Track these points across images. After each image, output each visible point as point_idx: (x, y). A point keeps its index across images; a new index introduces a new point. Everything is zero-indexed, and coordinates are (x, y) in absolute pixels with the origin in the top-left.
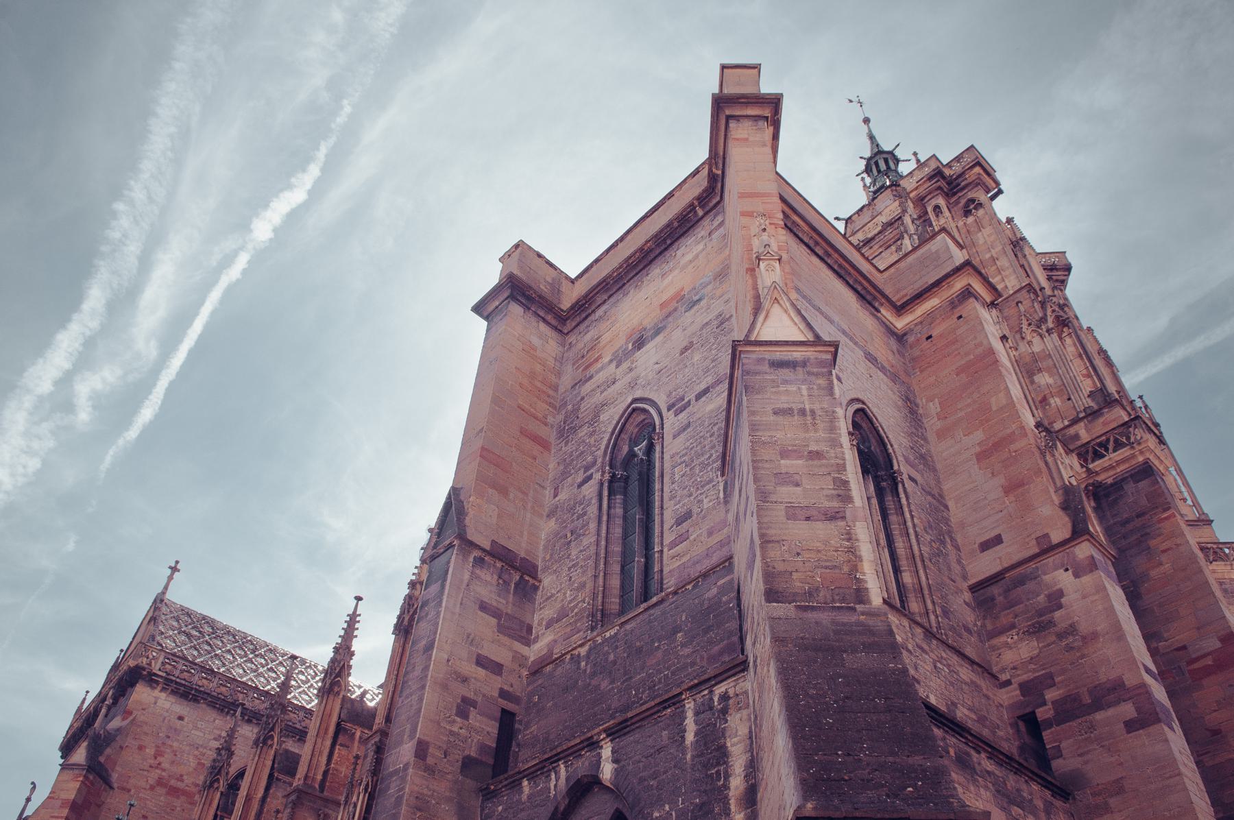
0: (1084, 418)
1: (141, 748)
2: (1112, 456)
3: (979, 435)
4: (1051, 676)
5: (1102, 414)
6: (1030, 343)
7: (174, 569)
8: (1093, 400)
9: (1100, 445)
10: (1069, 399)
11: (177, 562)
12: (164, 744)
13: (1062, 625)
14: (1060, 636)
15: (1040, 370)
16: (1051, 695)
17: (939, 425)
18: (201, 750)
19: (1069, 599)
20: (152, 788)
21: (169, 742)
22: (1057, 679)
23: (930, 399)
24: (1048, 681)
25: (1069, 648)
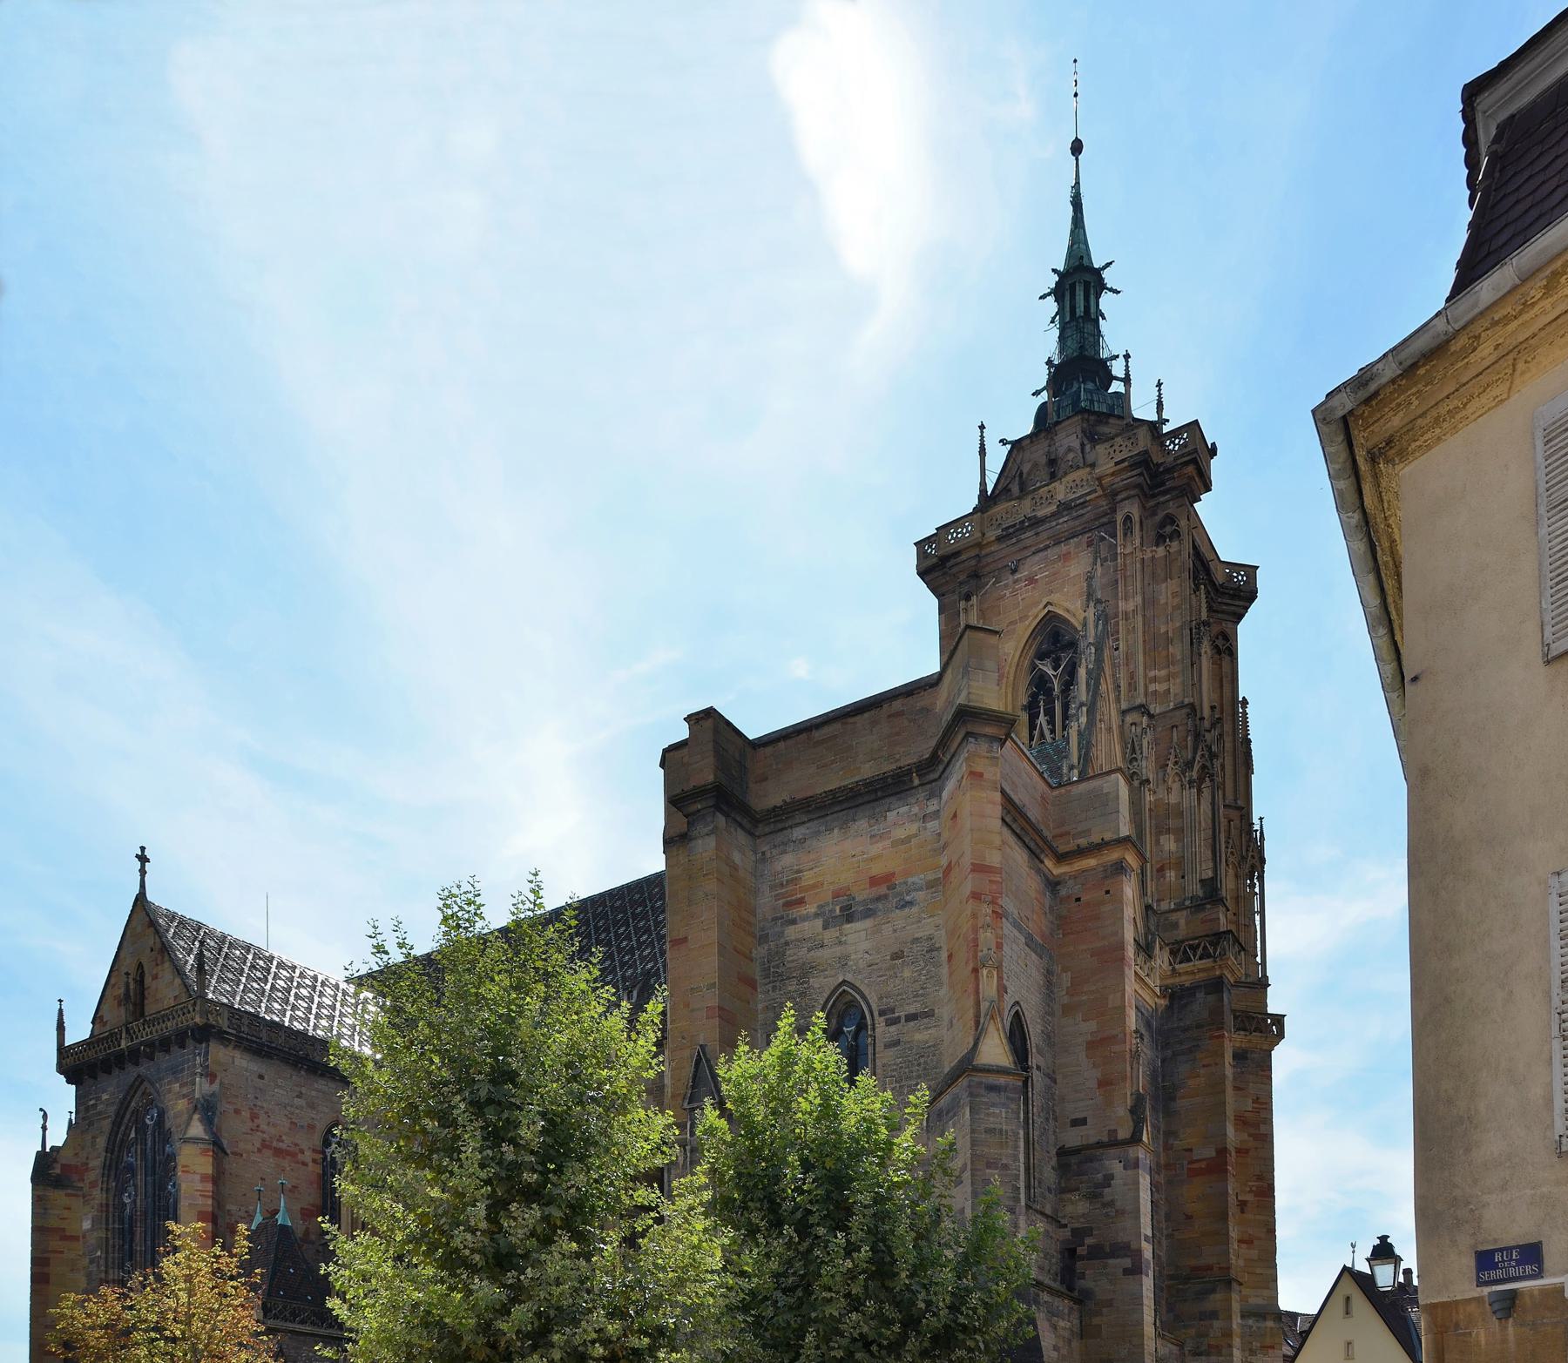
0: (1188, 907)
1: (237, 1112)
2: (1197, 963)
3: (1092, 1026)
4: (1091, 1229)
5: (1204, 909)
6: (1169, 790)
7: (143, 859)
8: (1202, 886)
9: (1191, 947)
10: (1183, 877)
11: (143, 849)
12: (255, 1105)
13: (1107, 1199)
14: (1105, 1205)
15: (1168, 831)
16: (1089, 1241)
17: (1066, 1000)
18: (288, 1108)
19: (1115, 1182)
20: (259, 1150)
21: (259, 1103)
22: (1095, 1233)
23: (1065, 970)
24: (1088, 1232)
25: (1107, 1215)
